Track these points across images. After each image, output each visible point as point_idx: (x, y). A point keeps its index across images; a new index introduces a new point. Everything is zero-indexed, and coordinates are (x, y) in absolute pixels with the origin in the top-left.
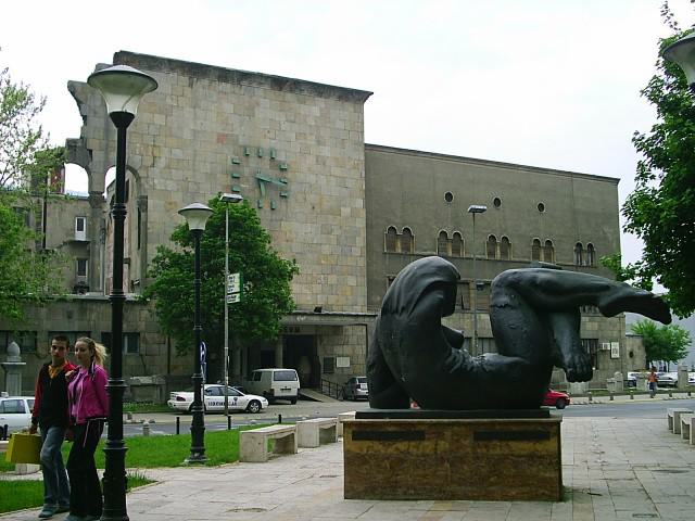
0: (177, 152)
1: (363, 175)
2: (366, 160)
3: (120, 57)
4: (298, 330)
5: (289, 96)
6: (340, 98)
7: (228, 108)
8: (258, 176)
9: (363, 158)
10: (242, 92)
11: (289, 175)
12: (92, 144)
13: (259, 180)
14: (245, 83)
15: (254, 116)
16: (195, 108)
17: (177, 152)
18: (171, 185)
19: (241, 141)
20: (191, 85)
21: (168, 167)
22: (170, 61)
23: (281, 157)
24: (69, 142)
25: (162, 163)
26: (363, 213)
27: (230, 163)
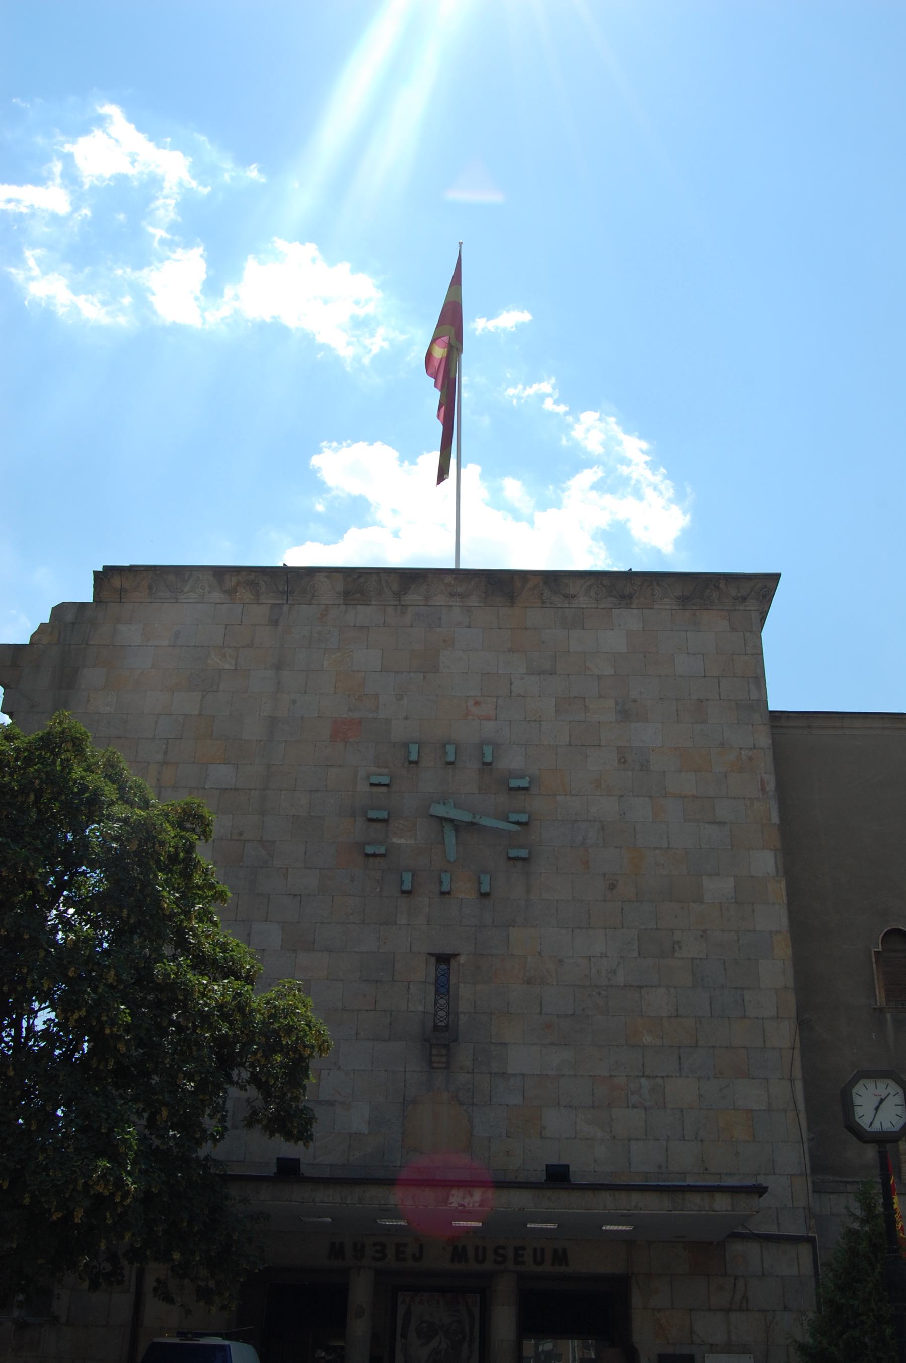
1: (771, 786)
2: (776, 746)
4: (561, 1257)
6: (684, 601)
8: (439, 810)
9: (764, 739)
13: (442, 819)
16: (278, 667)
22: (220, 572)
23: (512, 761)
26: (778, 890)
27: (362, 787)
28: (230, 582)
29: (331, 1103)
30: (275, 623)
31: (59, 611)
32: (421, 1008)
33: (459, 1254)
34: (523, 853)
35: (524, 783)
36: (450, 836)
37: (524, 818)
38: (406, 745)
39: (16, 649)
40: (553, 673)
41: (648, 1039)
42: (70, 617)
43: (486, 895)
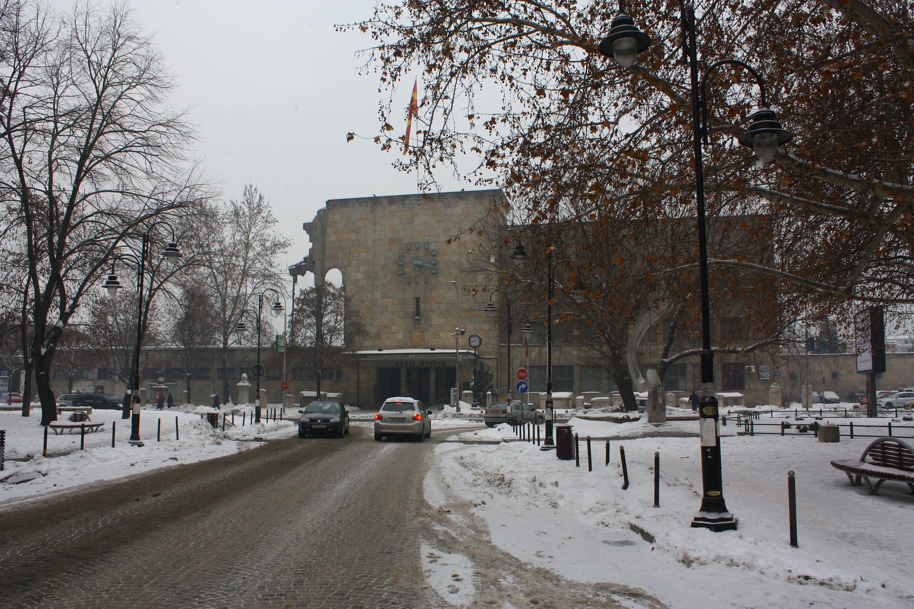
0: (363, 255)
3: (328, 202)
5: (439, 204)
7: (396, 220)
11: (439, 258)
12: (316, 258)
14: (407, 202)
16: (374, 225)
17: (363, 255)
18: (360, 276)
19: (404, 242)
20: (372, 212)
22: (357, 199)
23: (433, 247)
24: (305, 259)
25: (354, 263)
29: (394, 333)
30: (372, 212)
31: (319, 212)
33: (422, 363)
34: (435, 271)
36: (417, 269)
38: (406, 244)
39: (310, 223)
40: (442, 221)
41: (463, 315)
43: (426, 283)
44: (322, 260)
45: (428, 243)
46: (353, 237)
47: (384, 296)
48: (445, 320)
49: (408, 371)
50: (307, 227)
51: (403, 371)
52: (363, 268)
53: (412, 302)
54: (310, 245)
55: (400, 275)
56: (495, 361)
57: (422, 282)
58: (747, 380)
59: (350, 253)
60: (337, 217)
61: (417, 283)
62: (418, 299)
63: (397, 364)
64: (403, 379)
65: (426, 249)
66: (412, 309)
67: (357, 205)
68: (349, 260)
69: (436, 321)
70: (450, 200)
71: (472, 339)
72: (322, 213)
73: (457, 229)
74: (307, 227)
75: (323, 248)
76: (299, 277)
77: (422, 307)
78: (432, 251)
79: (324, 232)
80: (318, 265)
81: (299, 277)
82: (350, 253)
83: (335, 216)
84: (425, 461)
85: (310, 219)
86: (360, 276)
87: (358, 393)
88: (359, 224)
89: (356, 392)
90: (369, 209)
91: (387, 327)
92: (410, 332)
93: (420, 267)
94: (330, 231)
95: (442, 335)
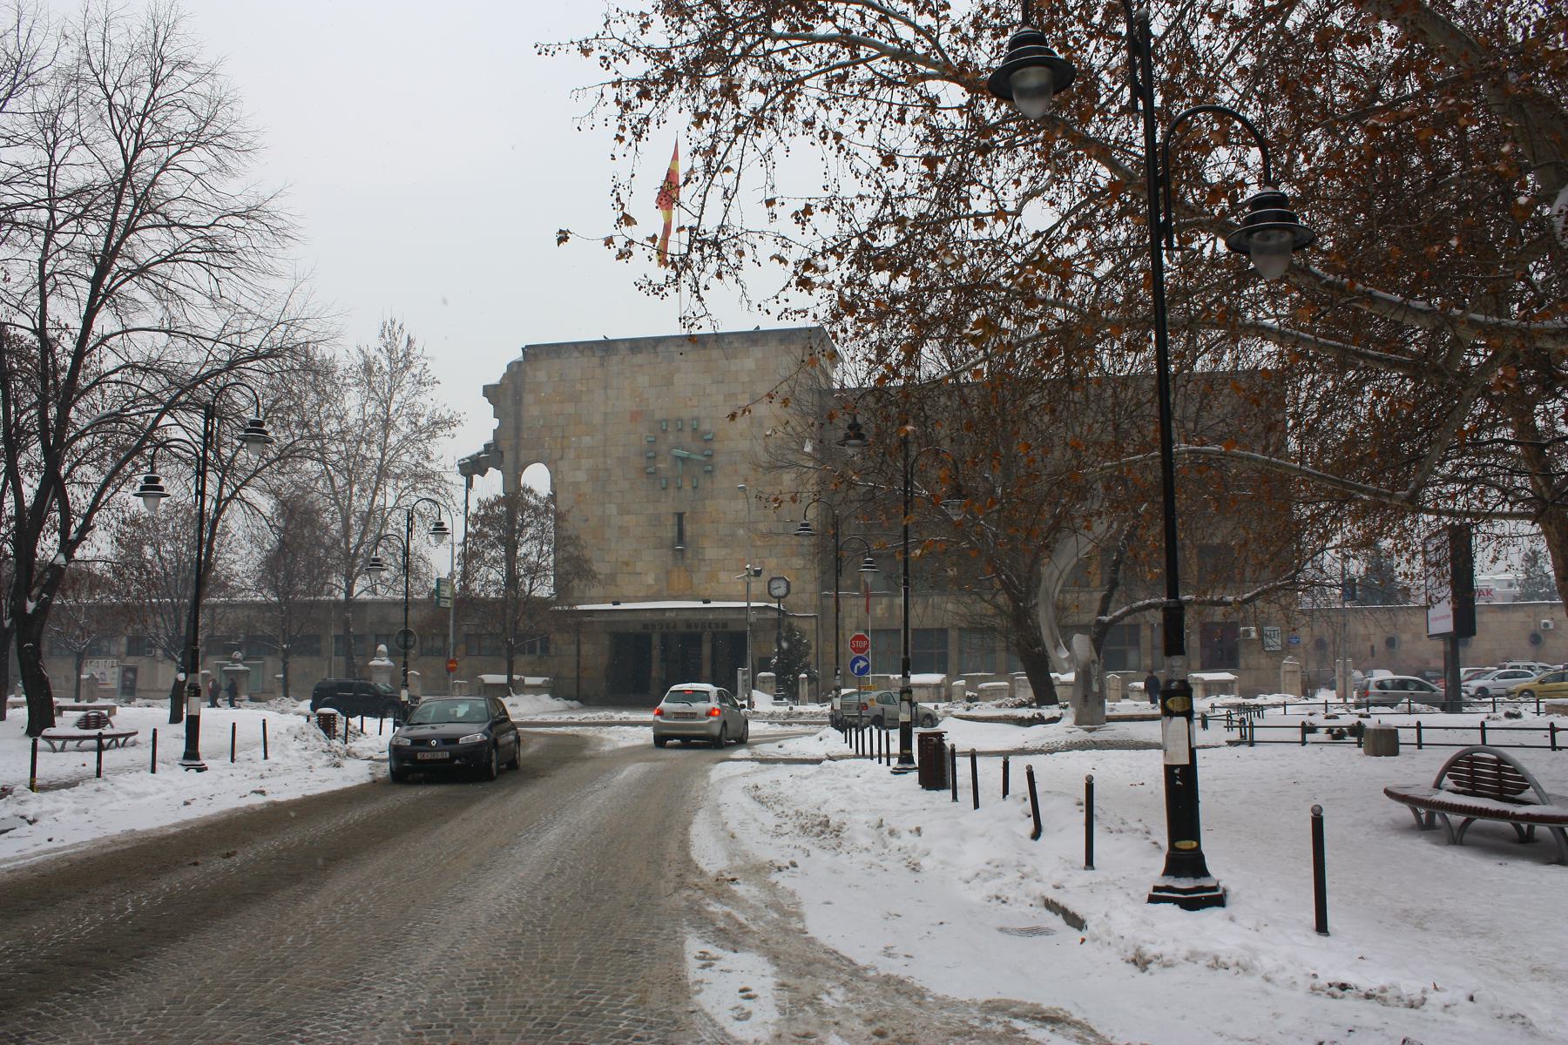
0: (587, 440)
5: (715, 353)
6: (782, 341)
7: (643, 380)
10: (659, 360)
11: (716, 446)
12: (505, 445)
14: (660, 348)
15: (672, 384)
16: (605, 388)
17: (587, 440)
18: (581, 476)
19: (658, 416)
21: (578, 457)
22: (576, 345)
23: (706, 426)
24: (487, 446)
25: (571, 454)
27: (644, 442)
28: (581, 347)
31: (510, 366)
32: (670, 535)
33: (689, 626)
34: (709, 468)
35: (709, 437)
36: (680, 464)
37: (710, 453)
38: (660, 422)
39: (495, 386)
40: (722, 382)
42: (515, 369)
43: (695, 488)
44: (516, 449)
45: (697, 419)
46: (569, 408)
47: (623, 511)
48: (728, 551)
49: (665, 638)
50: (490, 392)
51: (656, 640)
52: (586, 463)
53: (671, 522)
54: (496, 423)
55: (652, 475)
56: (814, 620)
57: (687, 487)
58: (1242, 650)
59: (563, 437)
60: (541, 374)
61: (679, 488)
62: (680, 516)
63: (645, 626)
64: (656, 653)
65: (695, 430)
66: (670, 533)
67: (576, 354)
68: (563, 449)
69: (711, 552)
70: (736, 345)
71: (774, 585)
72: (515, 369)
73: (747, 396)
74: (490, 392)
75: (518, 430)
76: (476, 477)
77: (689, 529)
78: (706, 433)
79: (518, 401)
80: (509, 457)
81: (476, 477)
82: (563, 437)
83: (538, 373)
84: (693, 794)
85: (495, 378)
86: (581, 476)
87: (578, 677)
88: (578, 386)
89: (574, 674)
90: (596, 361)
91: (627, 564)
92: (668, 573)
93: (683, 460)
94: (529, 398)
95: (723, 577)
